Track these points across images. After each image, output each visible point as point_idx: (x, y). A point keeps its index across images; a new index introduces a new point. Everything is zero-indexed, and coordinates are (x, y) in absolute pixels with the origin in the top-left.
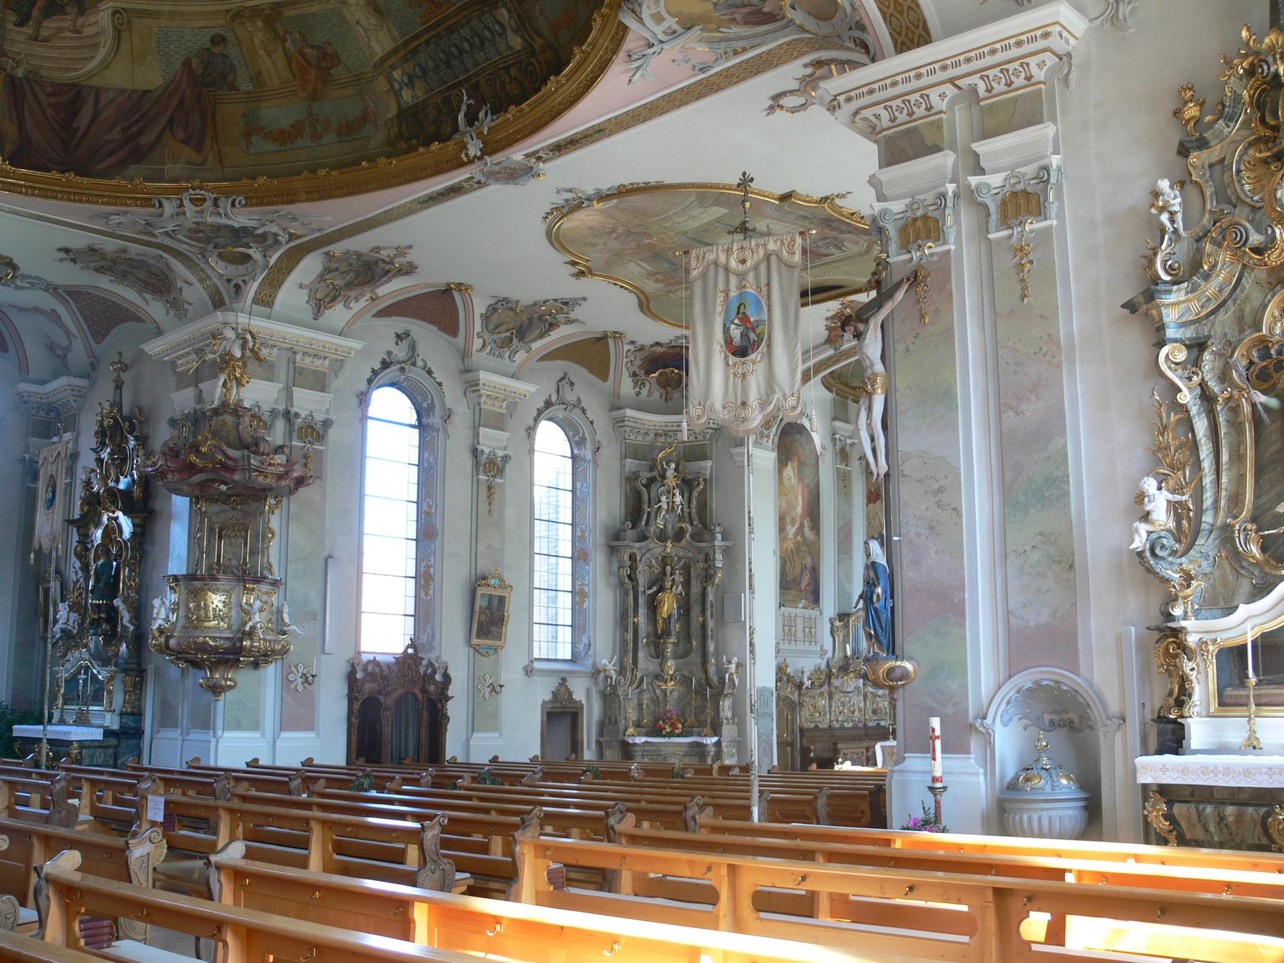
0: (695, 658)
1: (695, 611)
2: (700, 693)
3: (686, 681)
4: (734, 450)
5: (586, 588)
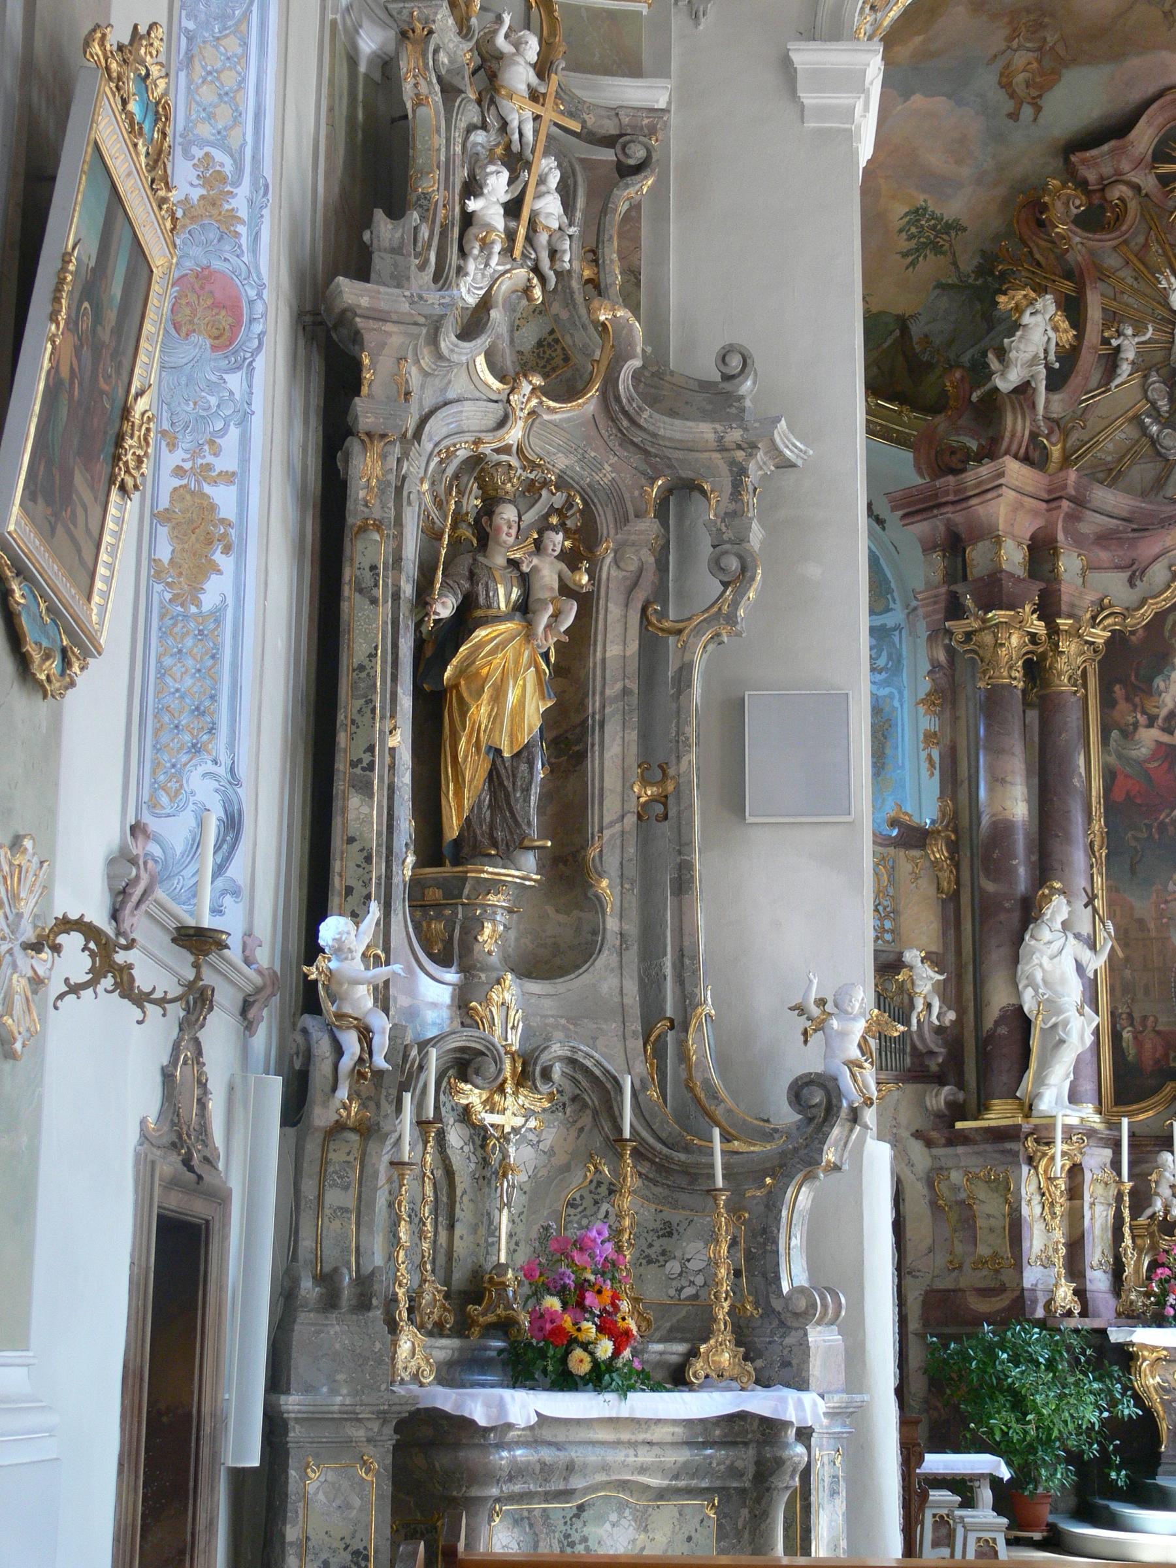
0: (609, 978)
1: (614, 753)
2: (672, 1168)
3: (589, 1098)
4: (805, 56)
5: (224, 498)
